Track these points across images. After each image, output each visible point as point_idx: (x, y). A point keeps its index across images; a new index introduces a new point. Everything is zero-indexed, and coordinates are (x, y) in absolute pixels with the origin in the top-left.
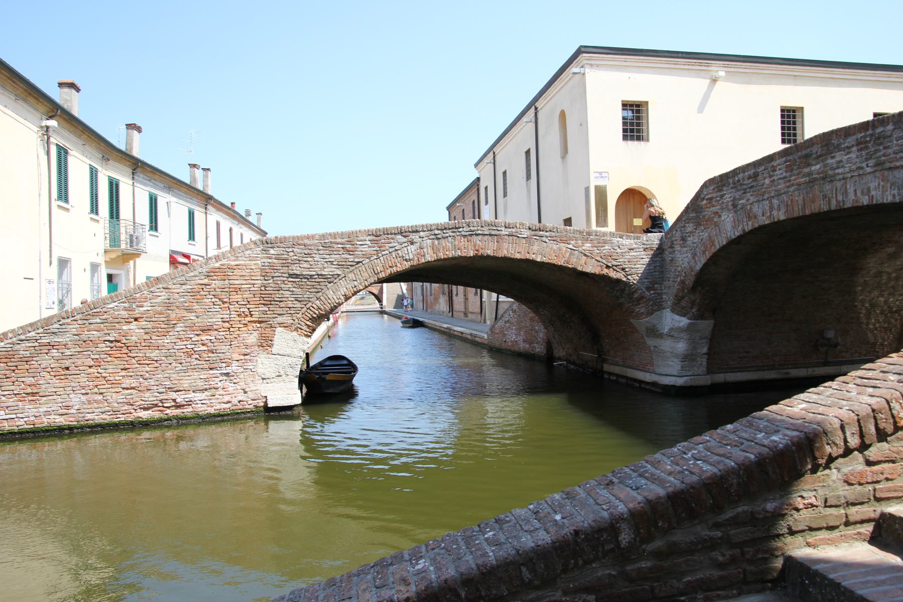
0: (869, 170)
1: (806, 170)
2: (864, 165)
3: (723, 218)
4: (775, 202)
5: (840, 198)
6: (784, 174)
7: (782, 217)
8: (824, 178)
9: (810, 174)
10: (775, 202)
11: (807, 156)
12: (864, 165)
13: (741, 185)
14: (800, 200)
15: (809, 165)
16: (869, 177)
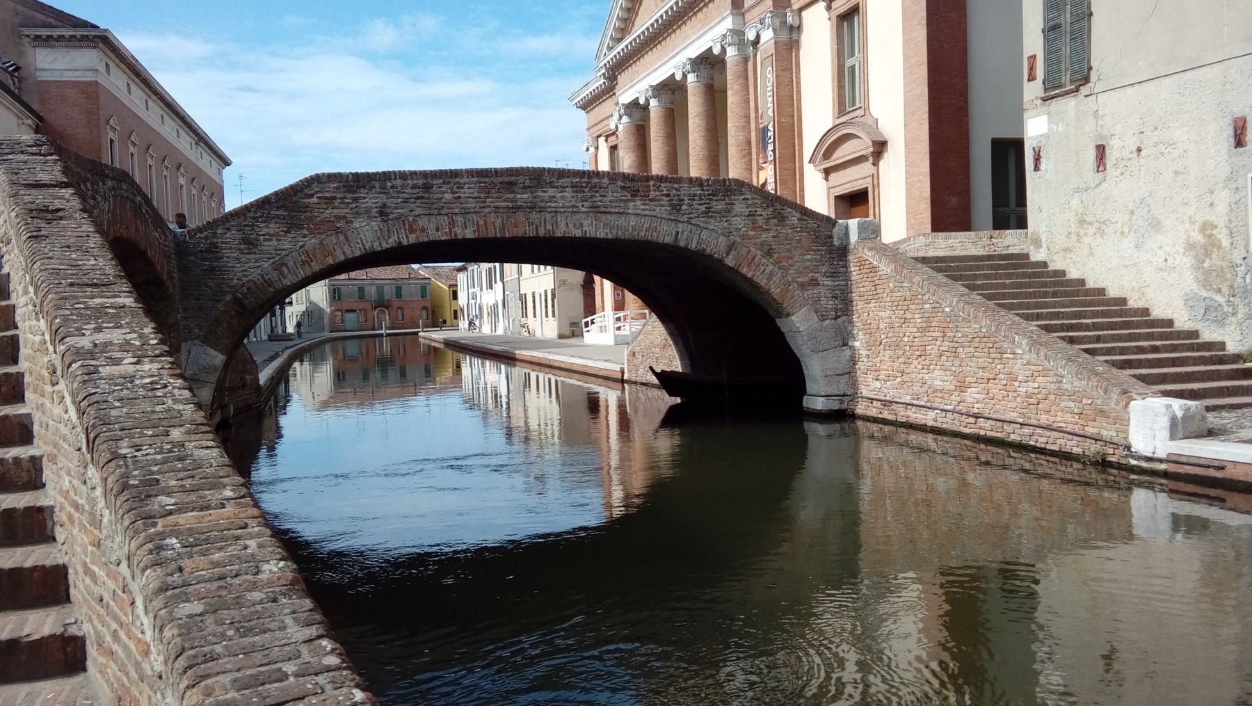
0: (584, 209)
1: (511, 196)
2: (580, 205)
3: (356, 225)
4: (459, 219)
5: (549, 227)
6: (476, 194)
7: (469, 234)
8: (531, 208)
9: (512, 201)
10: (459, 219)
11: (511, 183)
12: (580, 205)
13: (399, 192)
14: (498, 222)
15: (513, 192)
16: (583, 215)
